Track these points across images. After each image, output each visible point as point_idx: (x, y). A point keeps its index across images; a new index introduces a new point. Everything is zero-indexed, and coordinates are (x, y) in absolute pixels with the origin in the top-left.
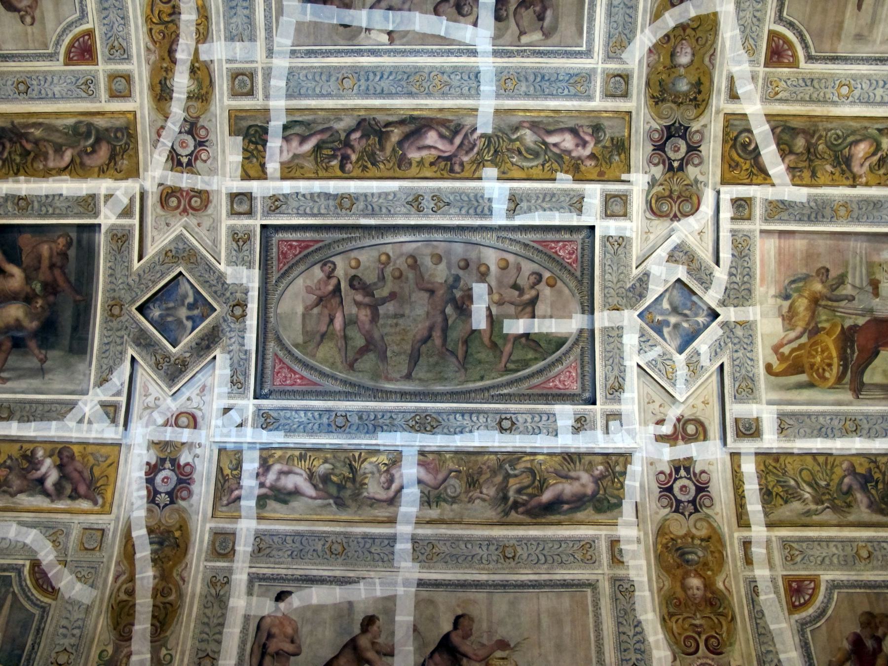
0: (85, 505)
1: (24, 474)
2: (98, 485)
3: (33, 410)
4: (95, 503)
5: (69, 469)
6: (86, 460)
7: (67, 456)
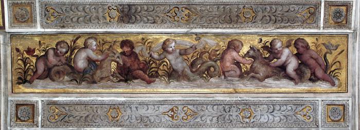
0: (322, 86)
1: (267, 62)
2: (333, 69)
3: (274, 11)
4: (333, 84)
5: (306, 57)
6: (319, 49)
7: (302, 47)
